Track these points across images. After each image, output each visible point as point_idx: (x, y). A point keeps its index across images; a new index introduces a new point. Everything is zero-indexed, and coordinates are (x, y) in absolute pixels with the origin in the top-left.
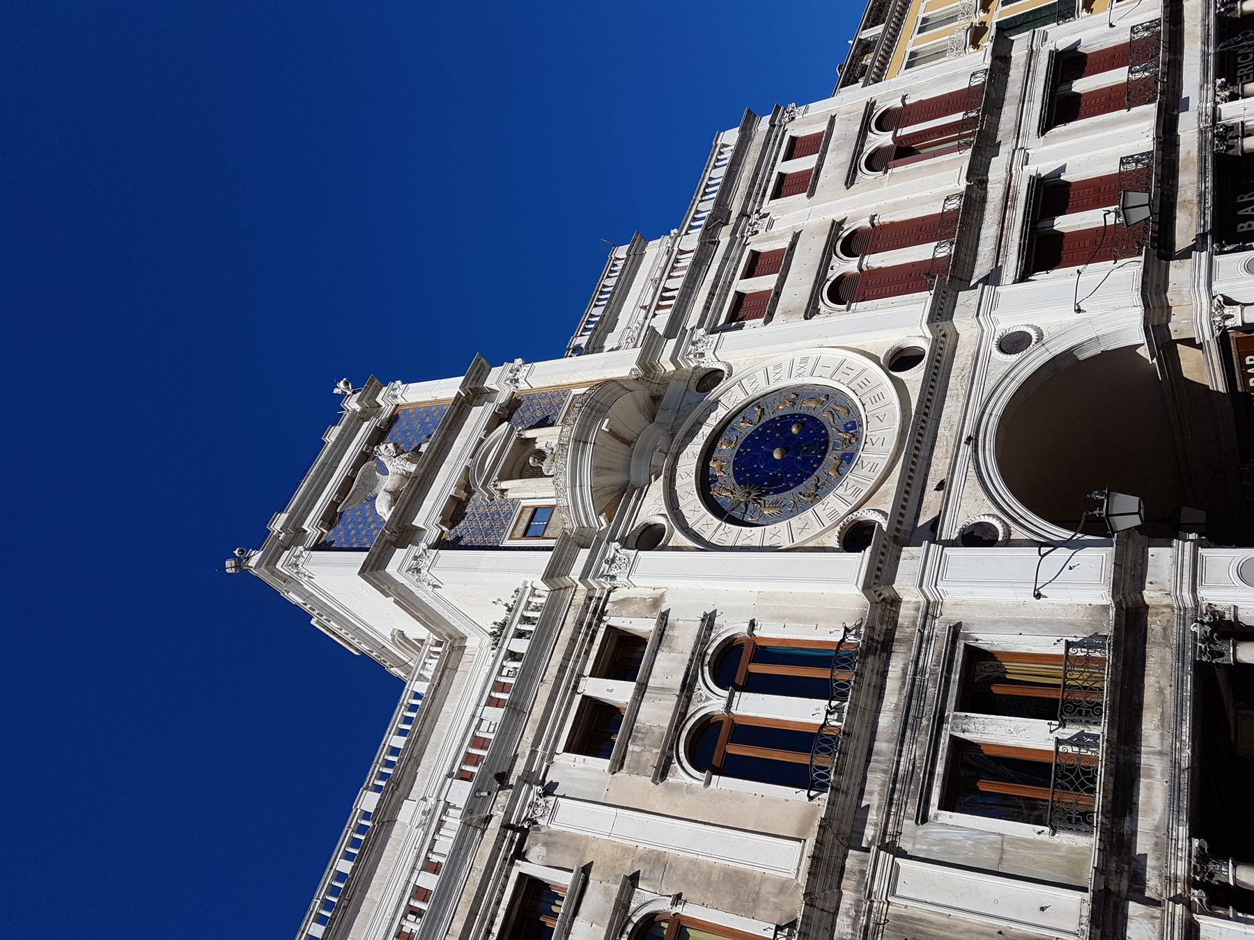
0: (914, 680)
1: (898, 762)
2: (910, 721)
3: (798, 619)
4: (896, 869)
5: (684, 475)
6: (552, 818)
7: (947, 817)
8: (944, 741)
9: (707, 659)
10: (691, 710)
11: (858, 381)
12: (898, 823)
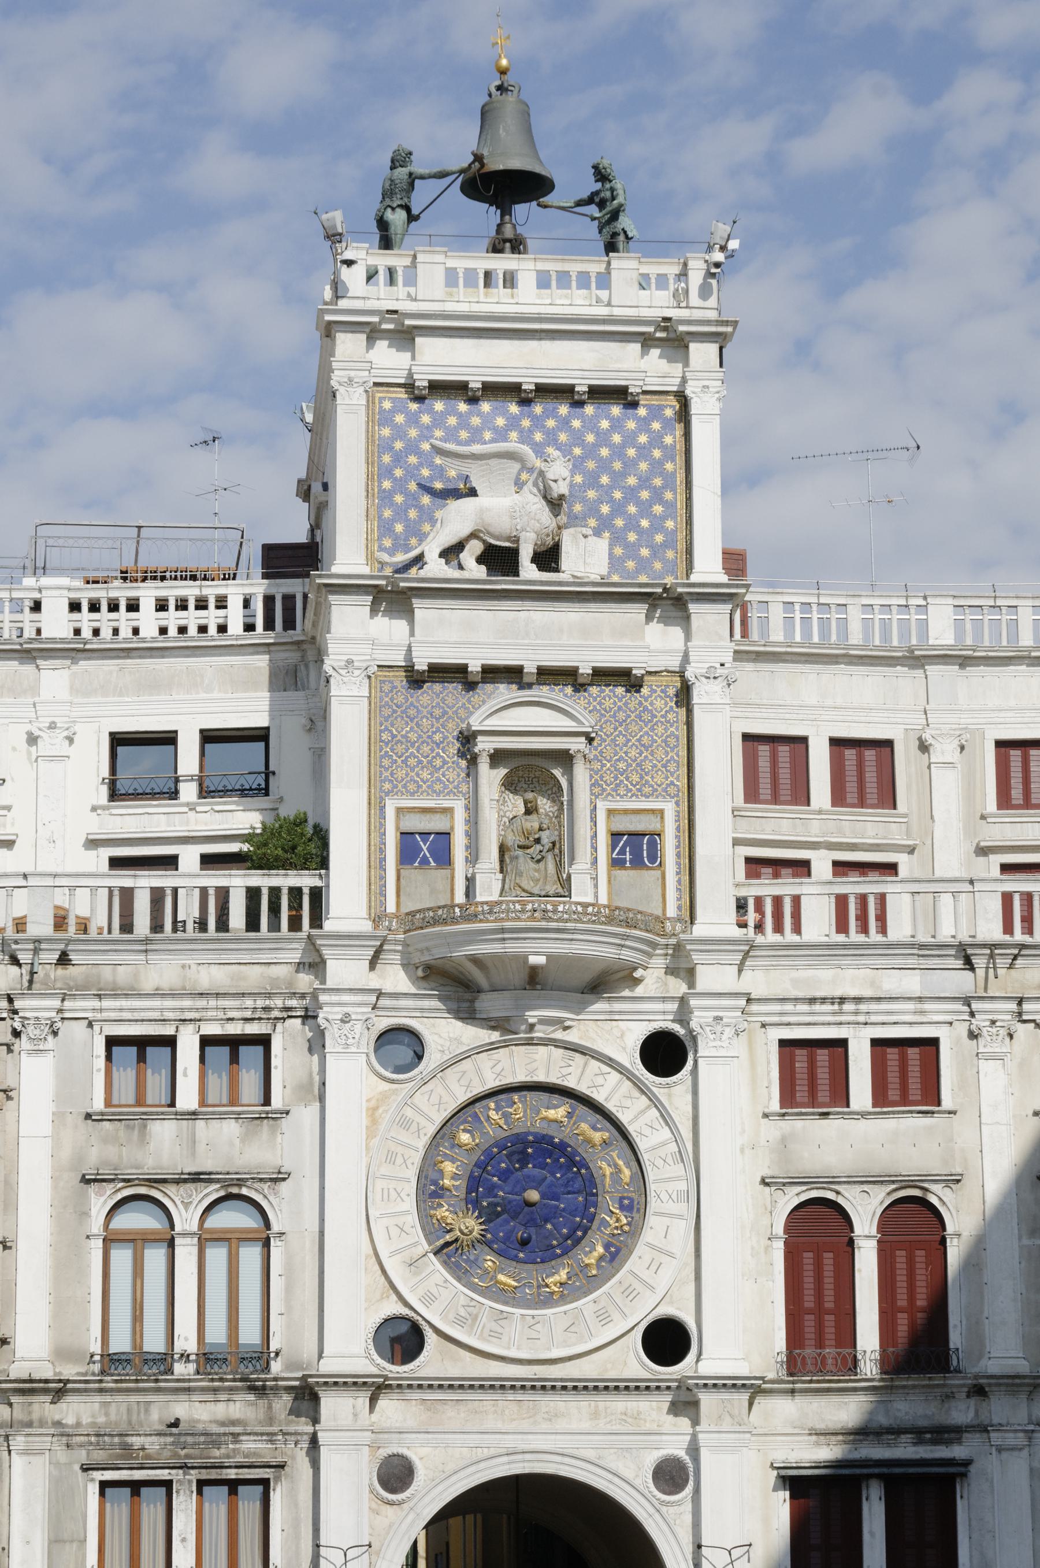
0: (225, 1434)
1: (139, 1435)
2: (183, 1439)
3: (289, 1289)
4: (40, 1452)
5: (498, 1068)
6: (30, 1052)
7: (94, 1490)
8: (163, 1474)
9: (235, 1190)
10: (171, 1189)
11: (636, 1284)
12: (81, 1445)
